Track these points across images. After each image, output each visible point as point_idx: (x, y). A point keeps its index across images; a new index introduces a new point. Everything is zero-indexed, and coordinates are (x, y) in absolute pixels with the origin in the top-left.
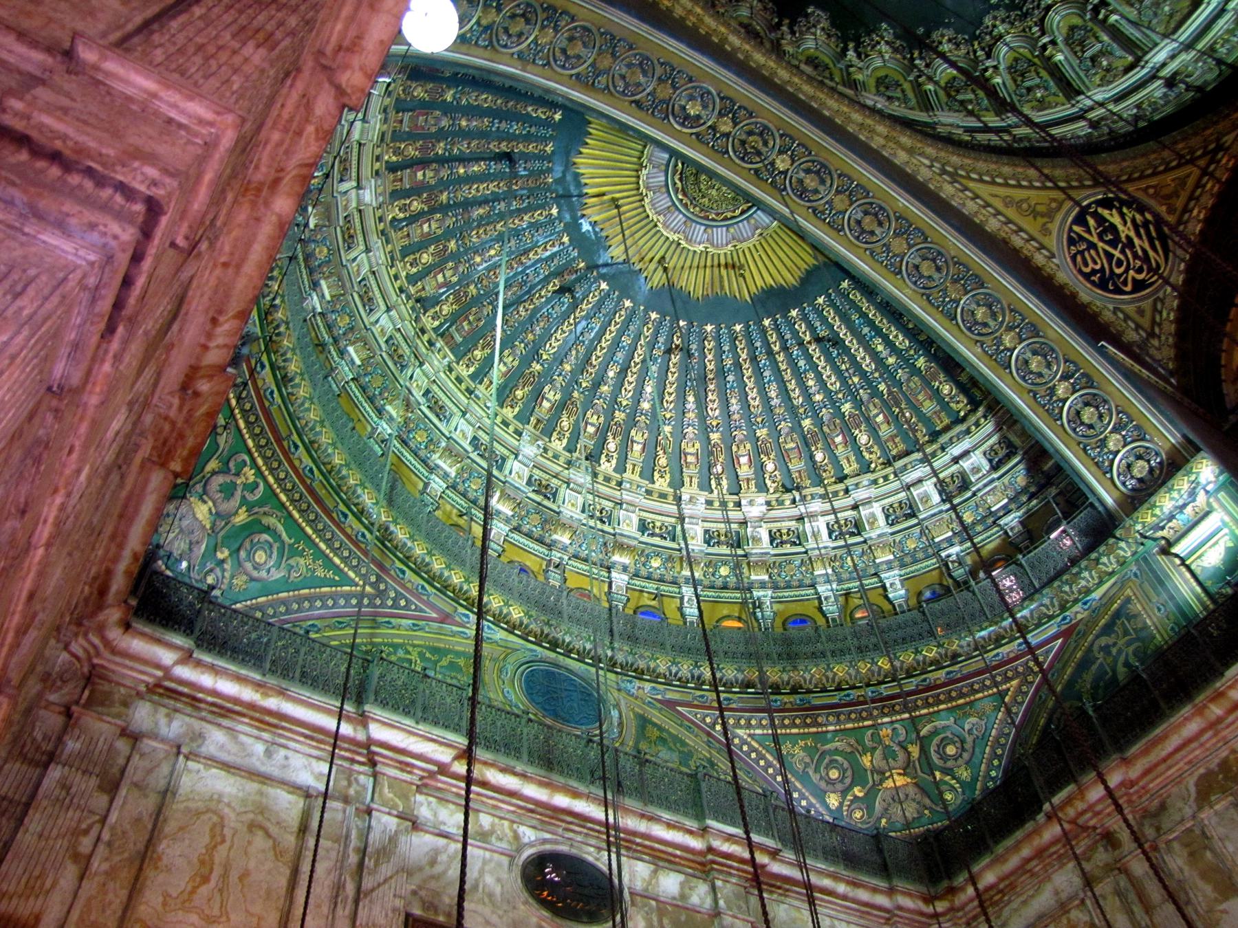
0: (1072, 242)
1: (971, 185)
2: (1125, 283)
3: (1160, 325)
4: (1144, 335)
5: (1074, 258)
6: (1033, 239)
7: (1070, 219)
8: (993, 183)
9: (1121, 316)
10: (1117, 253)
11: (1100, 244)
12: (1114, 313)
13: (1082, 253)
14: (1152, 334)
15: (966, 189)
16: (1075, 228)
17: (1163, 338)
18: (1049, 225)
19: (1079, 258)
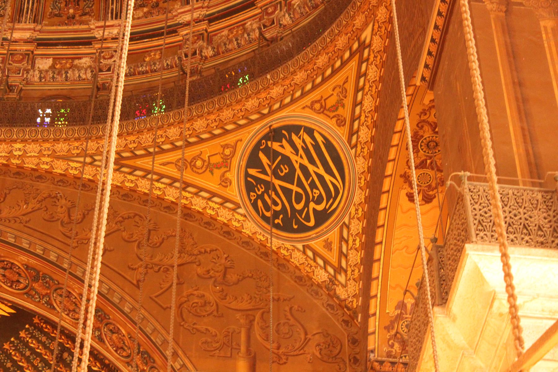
0: (250, 188)
1: (139, 163)
2: (308, 219)
3: (346, 256)
4: (331, 271)
5: (255, 205)
6: (214, 195)
7: (244, 164)
8: (163, 151)
9: (310, 254)
10: (295, 188)
11: (277, 182)
12: (304, 253)
13: (261, 197)
14: (339, 269)
15: (136, 169)
16: (252, 172)
17: (349, 272)
18: (228, 175)
19: (260, 203)
